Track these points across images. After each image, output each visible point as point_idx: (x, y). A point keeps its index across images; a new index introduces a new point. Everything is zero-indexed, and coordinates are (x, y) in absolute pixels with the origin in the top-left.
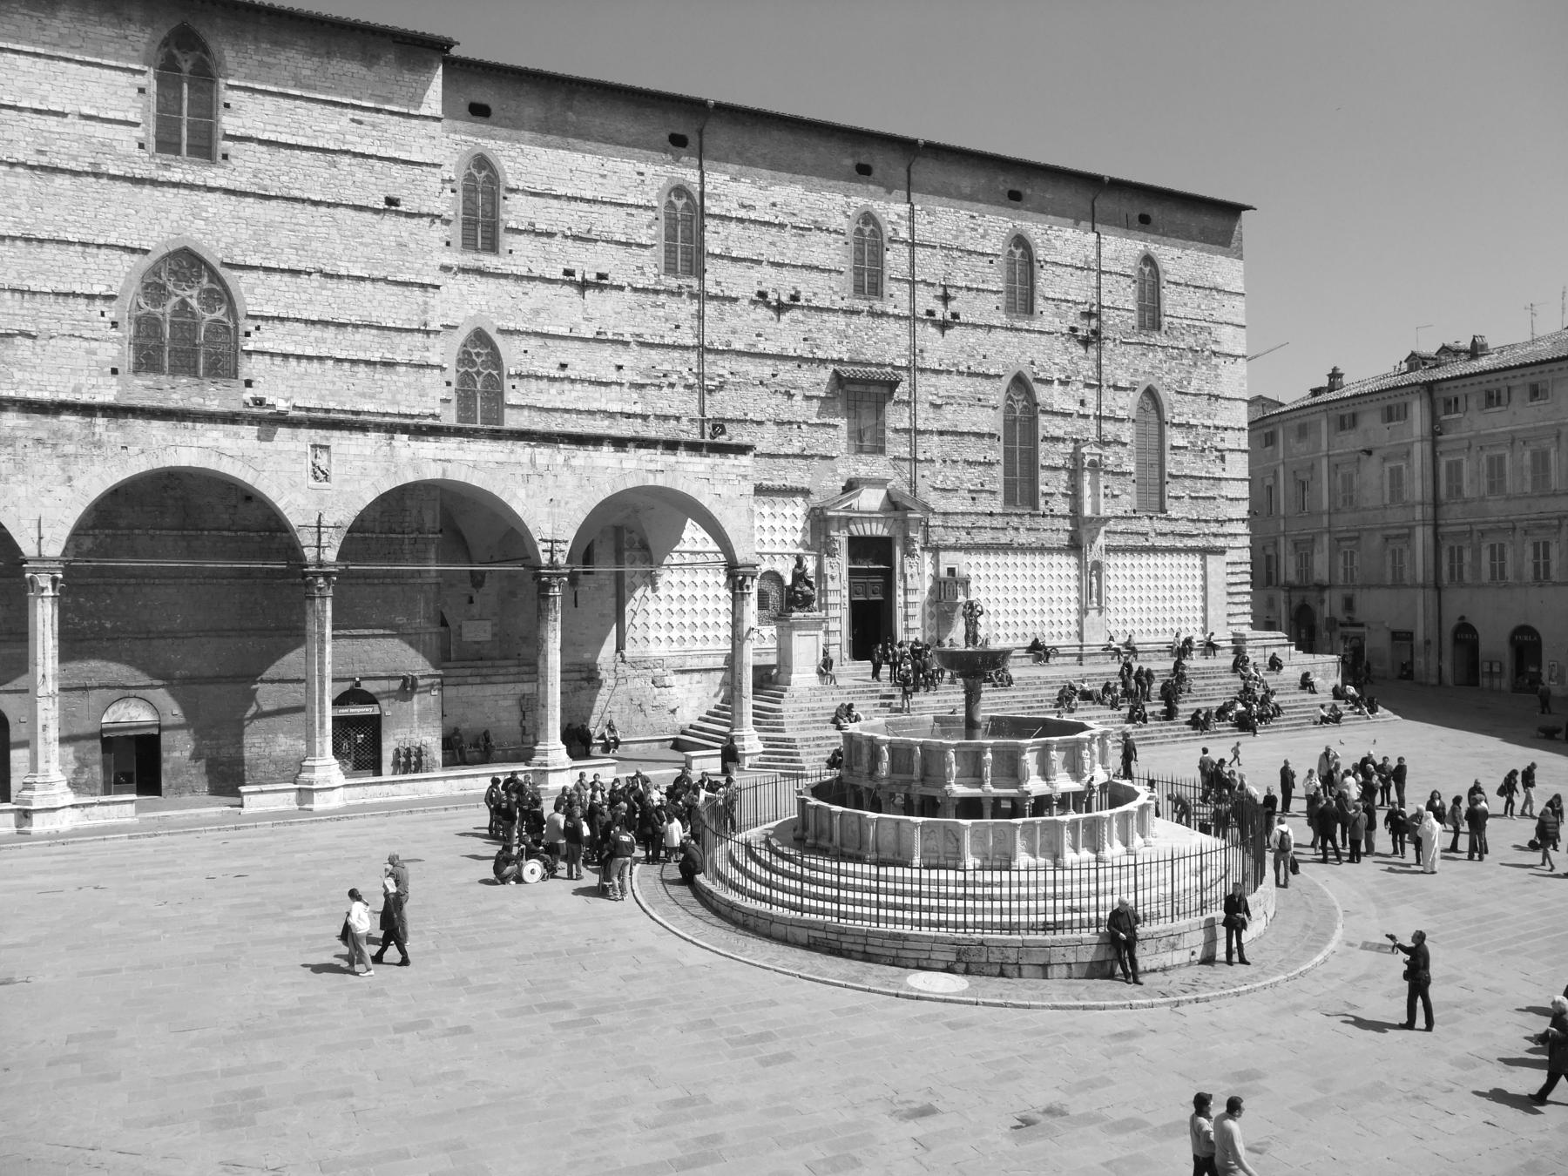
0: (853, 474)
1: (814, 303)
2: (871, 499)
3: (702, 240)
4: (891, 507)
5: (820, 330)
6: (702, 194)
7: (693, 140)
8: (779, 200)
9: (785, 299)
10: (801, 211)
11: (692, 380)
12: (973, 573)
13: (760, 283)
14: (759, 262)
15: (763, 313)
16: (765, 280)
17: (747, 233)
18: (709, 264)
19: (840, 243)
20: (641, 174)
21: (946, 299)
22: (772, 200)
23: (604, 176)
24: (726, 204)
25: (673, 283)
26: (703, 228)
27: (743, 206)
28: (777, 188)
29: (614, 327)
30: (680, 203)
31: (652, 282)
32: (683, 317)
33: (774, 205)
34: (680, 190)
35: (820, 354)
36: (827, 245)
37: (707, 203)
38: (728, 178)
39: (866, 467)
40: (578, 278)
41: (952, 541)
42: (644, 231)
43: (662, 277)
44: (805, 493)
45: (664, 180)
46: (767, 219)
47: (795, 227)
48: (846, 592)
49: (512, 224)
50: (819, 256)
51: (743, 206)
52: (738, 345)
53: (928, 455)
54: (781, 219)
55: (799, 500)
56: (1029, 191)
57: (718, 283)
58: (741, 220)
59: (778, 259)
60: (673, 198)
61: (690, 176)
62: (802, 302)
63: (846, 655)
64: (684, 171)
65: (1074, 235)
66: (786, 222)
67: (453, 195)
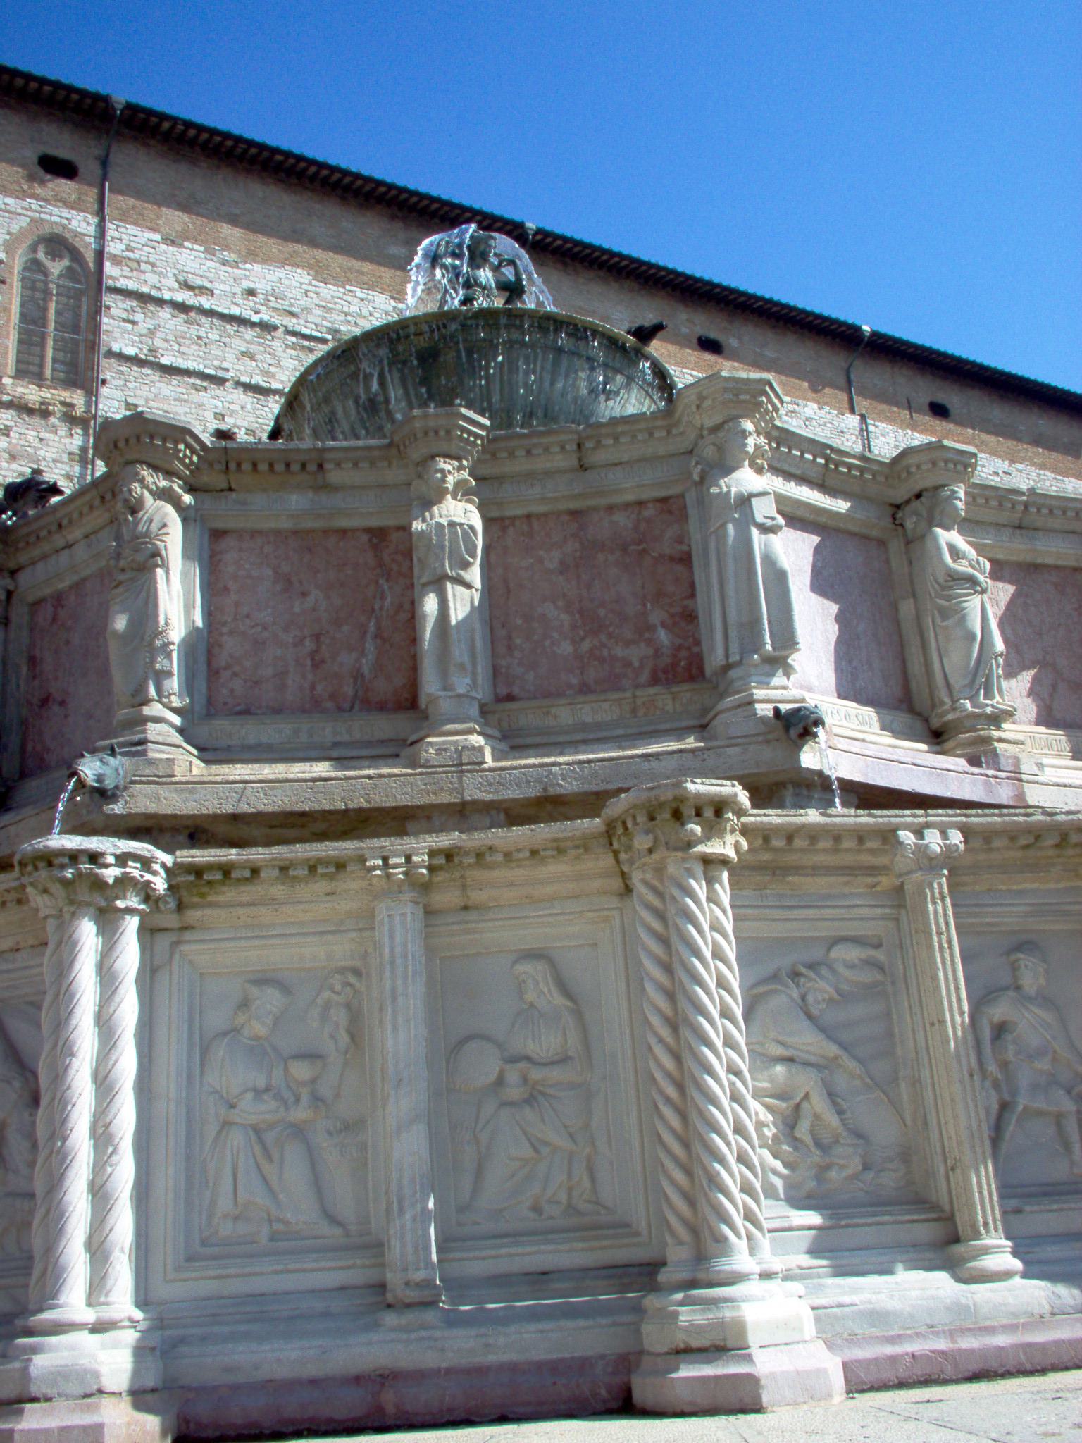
3: (96, 328)
6: (100, 255)
7: (89, 166)
8: (260, 286)
10: (306, 310)
13: (220, 417)
14: (219, 381)
16: (232, 414)
17: (194, 331)
18: (109, 370)
22: (246, 284)
24: (152, 278)
25: (31, 393)
26: (97, 310)
27: (186, 286)
28: (258, 267)
30: (56, 268)
32: (50, 456)
33: (251, 293)
34: (57, 243)
37: (109, 268)
38: (157, 237)
45: (24, 222)
46: (235, 311)
47: (294, 334)
51: (186, 286)
54: (265, 316)
56: (734, 342)
58: (182, 308)
59: (258, 380)
60: (41, 255)
61: (81, 224)
64: (65, 213)
65: (822, 413)
66: (276, 321)
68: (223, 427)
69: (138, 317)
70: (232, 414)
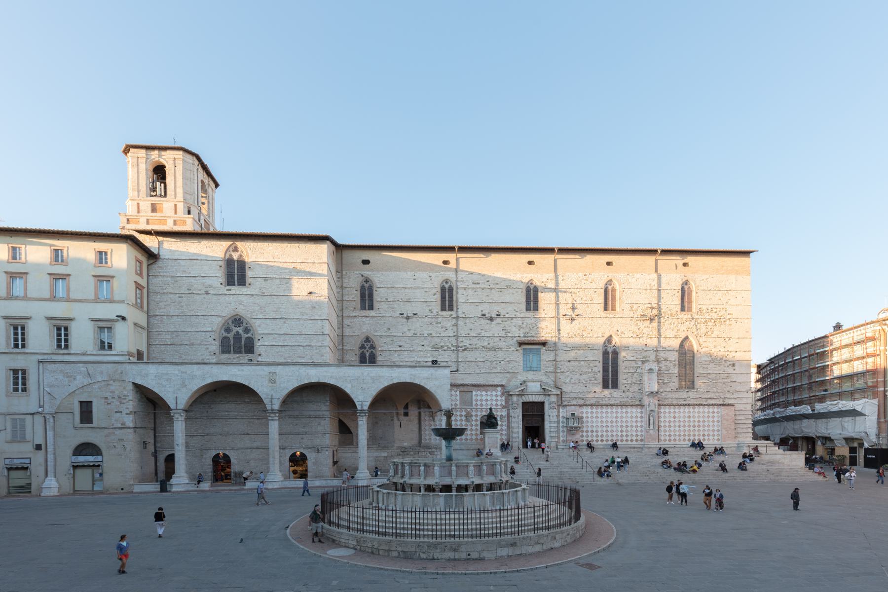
0: (526, 379)
1: (507, 316)
2: (534, 387)
4: (542, 391)
5: (510, 326)
9: (494, 316)
10: (501, 282)
11: (452, 348)
12: (584, 415)
13: (482, 311)
15: (483, 322)
19: (520, 293)
20: (431, 277)
21: (574, 308)
22: (487, 280)
23: (414, 279)
29: (420, 331)
31: (436, 314)
35: (509, 335)
36: (513, 294)
37: (459, 284)
39: (530, 376)
40: (405, 316)
41: (575, 403)
42: (432, 296)
43: (440, 312)
44: (502, 386)
48: (521, 423)
49: (379, 300)
50: (508, 298)
51: (473, 283)
52: (472, 334)
53: (562, 370)
55: (499, 389)
57: (464, 313)
59: (490, 301)
60: (444, 284)
62: (502, 316)
63: (521, 446)
64: (449, 273)
67: (356, 292)
68: (483, 313)
69: (464, 293)
70: (485, 309)
